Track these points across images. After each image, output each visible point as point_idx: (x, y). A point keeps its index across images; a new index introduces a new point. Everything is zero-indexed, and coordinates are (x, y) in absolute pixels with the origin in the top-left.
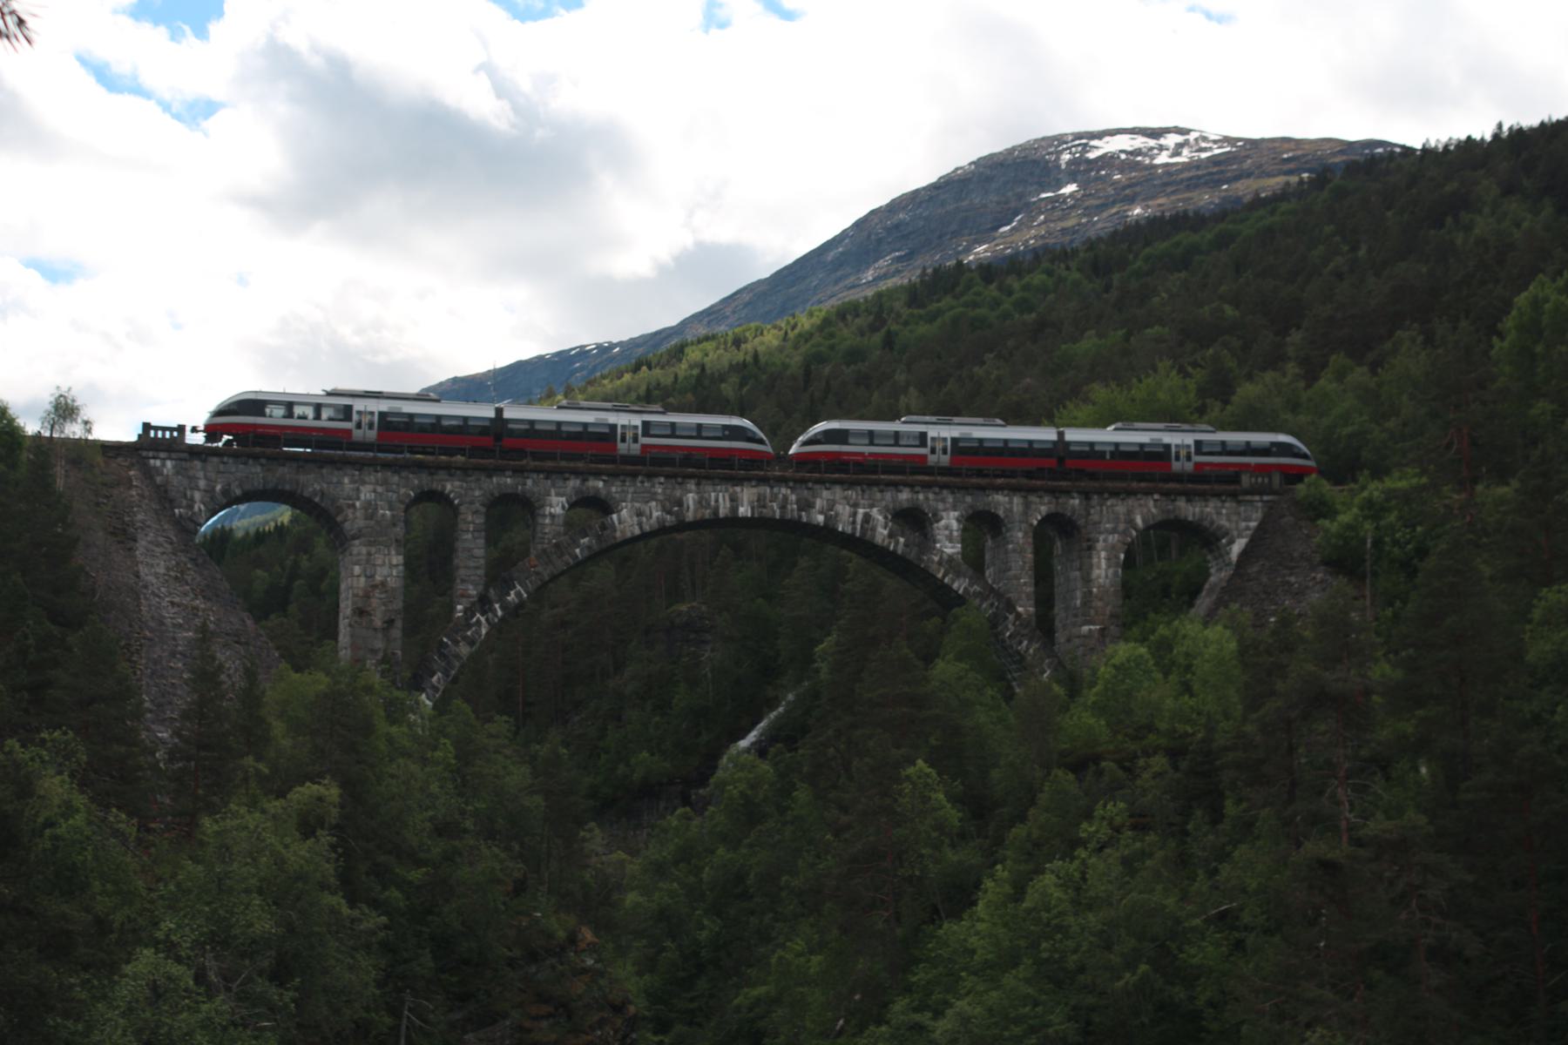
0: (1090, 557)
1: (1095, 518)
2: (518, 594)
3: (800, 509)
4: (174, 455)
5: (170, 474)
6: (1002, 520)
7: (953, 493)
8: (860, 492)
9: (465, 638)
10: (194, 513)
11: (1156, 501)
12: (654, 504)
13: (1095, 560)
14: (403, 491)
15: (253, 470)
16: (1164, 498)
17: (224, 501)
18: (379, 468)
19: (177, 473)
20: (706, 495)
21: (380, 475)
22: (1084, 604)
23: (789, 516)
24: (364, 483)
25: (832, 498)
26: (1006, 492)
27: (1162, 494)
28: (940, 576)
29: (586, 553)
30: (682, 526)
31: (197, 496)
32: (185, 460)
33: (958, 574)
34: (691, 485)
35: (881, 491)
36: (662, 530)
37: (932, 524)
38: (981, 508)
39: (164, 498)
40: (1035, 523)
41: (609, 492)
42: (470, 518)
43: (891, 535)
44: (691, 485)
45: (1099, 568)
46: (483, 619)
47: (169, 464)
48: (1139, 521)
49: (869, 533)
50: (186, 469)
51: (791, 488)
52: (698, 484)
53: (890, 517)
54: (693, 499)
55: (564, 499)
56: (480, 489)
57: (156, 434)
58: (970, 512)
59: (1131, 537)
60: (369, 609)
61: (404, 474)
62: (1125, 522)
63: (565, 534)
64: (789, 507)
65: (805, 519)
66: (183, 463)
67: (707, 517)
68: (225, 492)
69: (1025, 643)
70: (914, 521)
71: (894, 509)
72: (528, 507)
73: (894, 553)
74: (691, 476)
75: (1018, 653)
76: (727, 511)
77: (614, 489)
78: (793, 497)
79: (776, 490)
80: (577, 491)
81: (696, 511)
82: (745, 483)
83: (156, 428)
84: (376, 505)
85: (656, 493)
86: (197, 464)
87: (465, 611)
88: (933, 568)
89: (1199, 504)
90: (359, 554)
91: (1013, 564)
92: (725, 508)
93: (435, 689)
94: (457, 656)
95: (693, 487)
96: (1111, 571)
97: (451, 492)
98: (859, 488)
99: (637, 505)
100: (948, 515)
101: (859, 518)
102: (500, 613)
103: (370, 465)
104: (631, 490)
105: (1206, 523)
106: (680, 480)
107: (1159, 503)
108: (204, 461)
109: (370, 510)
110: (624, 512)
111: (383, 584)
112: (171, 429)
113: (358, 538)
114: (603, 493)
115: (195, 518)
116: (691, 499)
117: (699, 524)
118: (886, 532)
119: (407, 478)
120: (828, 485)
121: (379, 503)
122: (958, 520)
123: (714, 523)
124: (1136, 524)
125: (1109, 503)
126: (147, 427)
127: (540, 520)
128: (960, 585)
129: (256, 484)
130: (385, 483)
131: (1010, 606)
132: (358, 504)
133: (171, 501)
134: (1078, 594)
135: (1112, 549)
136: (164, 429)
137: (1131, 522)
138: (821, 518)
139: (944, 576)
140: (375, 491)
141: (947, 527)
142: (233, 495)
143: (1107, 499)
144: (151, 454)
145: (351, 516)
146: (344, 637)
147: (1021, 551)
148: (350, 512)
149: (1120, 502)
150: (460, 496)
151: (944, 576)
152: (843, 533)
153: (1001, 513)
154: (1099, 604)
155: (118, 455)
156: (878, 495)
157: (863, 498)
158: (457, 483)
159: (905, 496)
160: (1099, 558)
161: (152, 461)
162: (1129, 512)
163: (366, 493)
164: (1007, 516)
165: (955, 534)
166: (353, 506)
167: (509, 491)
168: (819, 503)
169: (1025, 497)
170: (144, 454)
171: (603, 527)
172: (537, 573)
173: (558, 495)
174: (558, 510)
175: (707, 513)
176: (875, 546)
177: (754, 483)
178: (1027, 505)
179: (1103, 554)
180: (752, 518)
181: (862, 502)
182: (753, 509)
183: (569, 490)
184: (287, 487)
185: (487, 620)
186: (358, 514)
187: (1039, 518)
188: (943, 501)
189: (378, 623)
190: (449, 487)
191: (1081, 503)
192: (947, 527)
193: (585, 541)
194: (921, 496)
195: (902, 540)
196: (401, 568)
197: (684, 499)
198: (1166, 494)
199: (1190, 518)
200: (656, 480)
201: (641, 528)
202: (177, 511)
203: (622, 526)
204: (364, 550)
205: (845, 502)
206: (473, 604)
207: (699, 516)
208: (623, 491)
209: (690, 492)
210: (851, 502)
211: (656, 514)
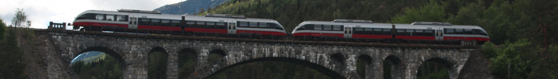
0: (405, 72)
1: (407, 57)
3: (296, 54)
4: (61, 34)
5: (60, 41)
6: (372, 58)
7: (353, 48)
8: (318, 48)
10: (69, 56)
11: (429, 51)
13: (407, 73)
14: (147, 47)
15: (91, 39)
16: (432, 50)
17: (80, 51)
18: (138, 39)
19: (63, 40)
20: (261, 49)
21: (139, 41)
23: (292, 57)
24: (133, 44)
25: (308, 50)
26: (373, 48)
27: (431, 48)
29: (216, 70)
30: (252, 60)
31: (70, 49)
32: (66, 36)
34: (255, 45)
35: (326, 47)
36: (244, 62)
37: (345, 59)
38: (364, 54)
39: (58, 50)
40: (384, 59)
41: (225, 48)
43: (330, 64)
44: (255, 45)
45: (408, 76)
47: (60, 37)
48: (423, 58)
49: (322, 63)
50: (66, 39)
51: (292, 46)
52: (258, 45)
53: (330, 57)
54: (256, 50)
55: (208, 50)
56: (176, 46)
57: (55, 26)
58: (360, 55)
59: (420, 64)
62: (418, 59)
63: (208, 63)
64: (292, 53)
65: (298, 58)
66: (65, 37)
67: (261, 57)
68: (81, 48)
70: (339, 58)
71: (331, 54)
72: (194, 53)
73: (331, 70)
74: (255, 42)
76: (269, 55)
77: (226, 47)
78: (293, 50)
79: (287, 47)
80: (213, 47)
81: (257, 55)
82: (276, 44)
83: (55, 24)
84: (137, 52)
85: (242, 48)
86: (70, 37)
88: (346, 76)
89: (445, 52)
90: (131, 71)
91: (376, 74)
92: (268, 53)
95: (256, 46)
96: (412, 77)
98: (318, 46)
99: (235, 52)
100: (351, 56)
101: (318, 57)
103: (135, 38)
104: (233, 47)
105: (448, 59)
107: (430, 52)
108: (73, 36)
109: (135, 54)
110: (230, 55)
112: (61, 24)
113: (131, 65)
114: (222, 48)
115: (69, 57)
116: (255, 50)
117: (258, 60)
118: (328, 63)
119: (149, 43)
120: (306, 45)
121: (138, 52)
122: (355, 58)
123: (264, 59)
124: (422, 60)
125: (412, 52)
126: (51, 23)
127: (199, 58)
129: (92, 45)
130: (141, 44)
132: (130, 52)
133: (60, 51)
135: (413, 69)
136: (58, 24)
137: (420, 59)
138: (304, 57)
140: (137, 47)
141: (351, 61)
142: (84, 49)
143: (411, 50)
144: (53, 33)
145: (128, 56)
147: (379, 70)
148: (127, 55)
149: (416, 51)
150: (168, 49)
152: (312, 63)
153: (371, 55)
155: (41, 34)
156: (325, 49)
157: (319, 50)
158: (168, 44)
159: (335, 49)
160: (408, 72)
161: (53, 36)
162: (419, 55)
164: (373, 57)
165: (354, 63)
166: (129, 53)
167: (187, 47)
168: (303, 52)
169: (380, 50)
170: (50, 33)
171: (222, 61)
173: (205, 49)
174: (205, 54)
175: (261, 56)
176: (324, 68)
177: (279, 44)
178: (381, 53)
179: (409, 71)
180: (278, 57)
181: (319, 51)
182: (278, 54)
184: (104, 46)
186: (131, 56)
187: (386, 57)
188: (350, 51)
190: (164, 46)
191: (401, 52)
192: (351, 61)
193: (216, 65)
194: (341, 49)
195: (334, 65)
196: (147, 76)
197: (253, 50)
198: (433, 48)
199: (442, 57)
200: (242, 43)
202: (63, 55)
203: (229, 60)
204: (133, 69)
205: (313, 51)
207: (258, 56)
209: (255, 47)
210: (315, 51)
211: (242, 56)
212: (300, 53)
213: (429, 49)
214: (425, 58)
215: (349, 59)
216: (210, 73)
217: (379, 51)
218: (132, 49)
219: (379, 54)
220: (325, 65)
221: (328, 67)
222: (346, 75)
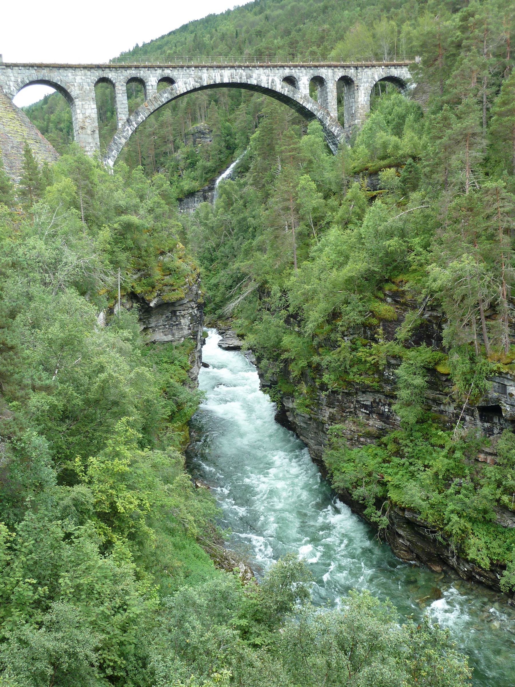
0: (358, 93)
1: (360, 77)
3: (247, 78)
9: (123, 136)
13: (360, 94)
14: (92, 78)
23: (243, 82)
24: (77, 75)
28: (301, 103)
29: (166, 100)
30: (202, 88)
31: (12, 84)
33: (308, 102)
34: (205, 70)
36: (195, 90)
43: (282, 88)
55: (156, 78)
65: (249, 83)
73: (284, 95)
74: (205, 67)
77: (175, 73)
87: (122, 125)
93: (114, 157)
96: (366, 98)
99: (184, 79)
101: (270, 81)
102: (136, 126)
104: (182, 73)
105: (402, 78)
118: (280, 86)
127: (147, 87)
128: (309, 106)
130: (85, 75)
131: (328, 114)
132: (75, 84)
137: (373, 78)
148: (72, 88)
153: (324, 77)
154: (362, 111)
158: (114, 74)
163: (78, 79)
171: (172, 90)
172: (148, 109)
173: (153, 77)
175: (212, 82)
179: (363, 92)
183: (157, 75)
188: (302, 72)
189: (89, 132)
194: (293, 71)
196: (96, 110)
198: (387, 66)
200: (191, 69)
204: (80, 103)
213: (383, 67)
216: (161, 104)
218: (77, 81)
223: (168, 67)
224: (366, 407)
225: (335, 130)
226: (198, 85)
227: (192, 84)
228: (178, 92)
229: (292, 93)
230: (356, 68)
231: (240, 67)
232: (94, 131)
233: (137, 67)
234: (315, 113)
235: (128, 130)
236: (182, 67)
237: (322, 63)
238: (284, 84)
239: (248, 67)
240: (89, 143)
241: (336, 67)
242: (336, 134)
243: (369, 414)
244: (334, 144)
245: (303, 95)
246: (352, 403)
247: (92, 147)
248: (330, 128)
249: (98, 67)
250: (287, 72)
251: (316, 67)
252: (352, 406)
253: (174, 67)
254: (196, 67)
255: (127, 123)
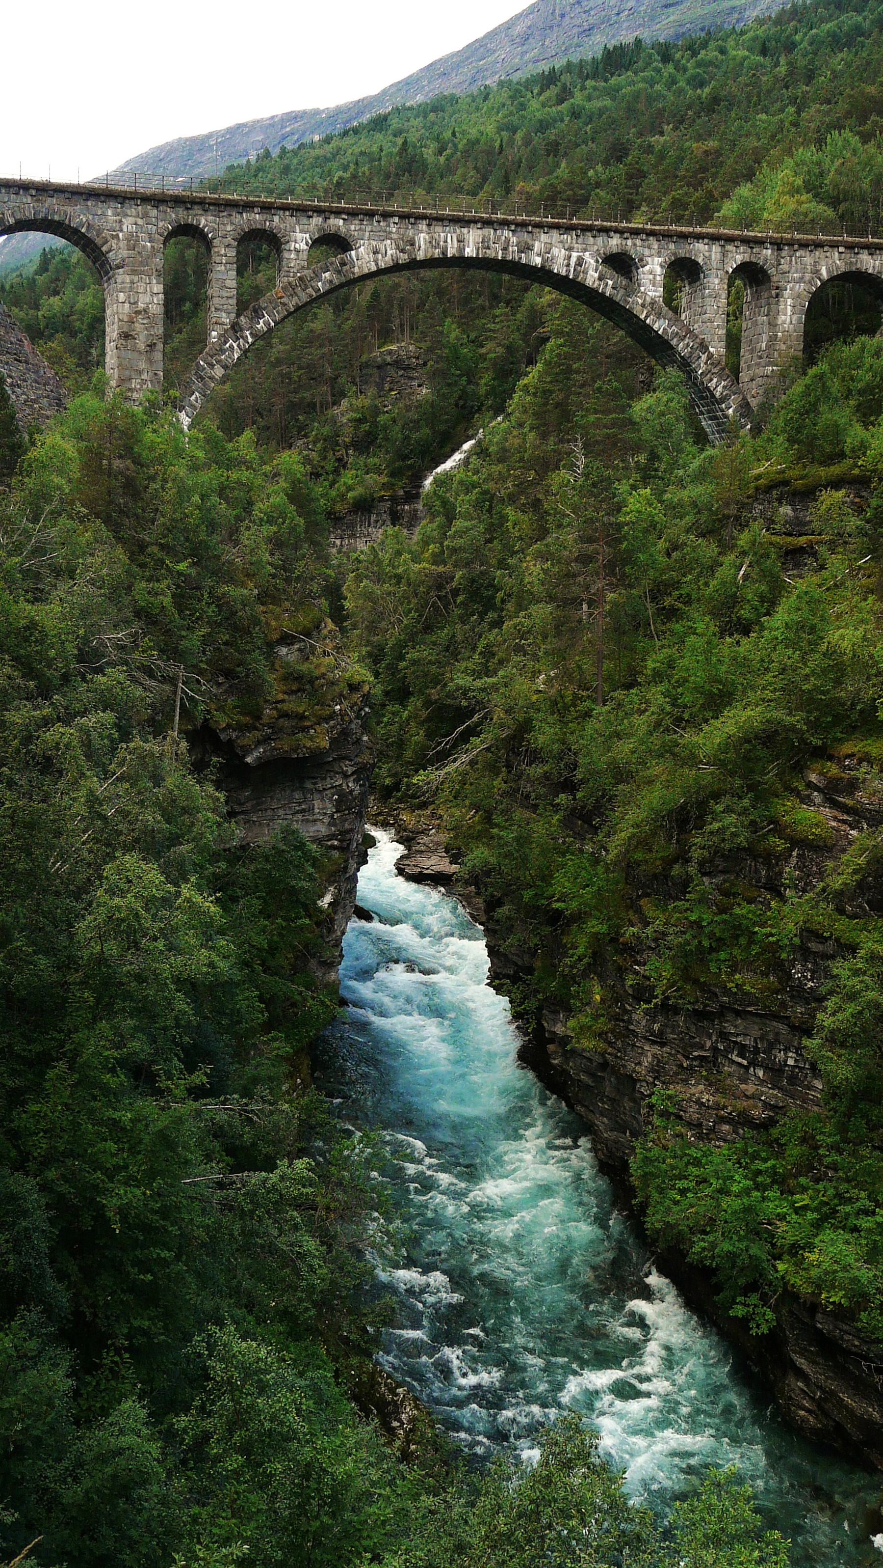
1: (785, 267)
2: (267, 323)
7: (658, 240)
9: (218, 362)
12: (389, 242)
20: (436, 235)
22: (768, 347)
26: (706, 241)
28: (642, 317)
29: (328, 287)
30: (414, 265)
33: (659, 316)
34: (423, 225)
35: (594, 237)
36: (396, 268)
40: (731, 270)
41: (349, 230)
42: (223, 252)
44: (423, 225)
45: (785, 315)
46: (235, 345)
48: (824, 272)
52: (429, 225)
56: (232, 223)
60: (133, 333)
61: (161, 208)
63: (308, 268)
65: (524, 261)
67: (436, 256)
69: (715, 380)
73: (603, 294)
74: (424, 217)
75: (708, 388)
76: (454, 251)
77: (353, 227)
78: (514, 240)
81: (426, 251)
85: (391, 232)
87: (220, 336)
88: (637, 310)
93: (195, 408)
94: (211, 378)
95: (424, 227)
96: (795, 317)
97: (205, 227)
99: (374, 243)
101: (573, 261)
102: (250, 340)
103: (129, 199)
104: (369, 228)
106: (412, 220)
109: (132, 242)
110: (362, 249)
111: (145, 311)
114: (343, 230)
116: (422, 238)
117: (430, 263)
118: (596, 275)
119: (165, 212)
123: (443, 262)
125: (798, 254)
127: (286, 255)
128: (660, 326)
130: (145, 216)
131: (703, 347)
132: (121, 235)
134: (765, 337)
137: (817, 272)
139: (647, 317)
145: (114, 246)
146: (111, 359)
150: (214, 230)
151: (647, 317)
152: (558, 275)
154: (783, 347)
159: (615, 243)
163: (128, 225)
165: (658, 278)
167: (259, 227)
169: (723, 246)
172: (284, 304)
173: (301, 232)
174: (303, 246)
175: (437, 253)
177: (479, 225)
178: (724, 254)
180: (477, 258)
182: (478, 249)
183: (312, 227)
184: (56, 218)
185: (239, 346)
188: (649, 248)
189: (142, 346)
190: (203, 222)
191: (772, 254)
193: (327, 274)
194: (629, 242)
195: (610, 283)
196: (161, 296)
198: (850, 247)
199: (870, 271)
200: (392, 220)
201: (377, 264)
203: (360, 262)
204: (128, 279)
205: (561, 245)
206: (226, 331)
208: (360, 229)
209: (422, 232)
212: (529, 248)
213: (841, 249)
214: (828, 271)
215: (647, 268)
217: (719, 249)
219: (719, 256)
220: (589, 282)
221: (595, 285)
222: (639, 308)
223: (338, 213)
224: (743, 1050)
225: (717, 385)
226: (403, 258)
227: (390, 253)
228: (356, 270)
229: (622, 292)
230: (778, 245)
231: (505, 223)
232: (152, 346)
233: (266, 208)
234: (674, 342)
235: (231, 347)
236: (371, 214)
237: (698, 229)
238: (609, 272)
239: (523, 225)
240: (140, 373)
241: (730, 239)
242: (718, 395)
243: (747, 1068)
244: (711, 419)
245: (648, 299)
246: (710, 1037)
247: (144, 382)
248: (705, 380)
249: (177, 201)
250: (615, 243)
251: (684, 236)
252: (708, 1044)
253: (353, 214)
254: (403, 217)
255: (231, 332)
